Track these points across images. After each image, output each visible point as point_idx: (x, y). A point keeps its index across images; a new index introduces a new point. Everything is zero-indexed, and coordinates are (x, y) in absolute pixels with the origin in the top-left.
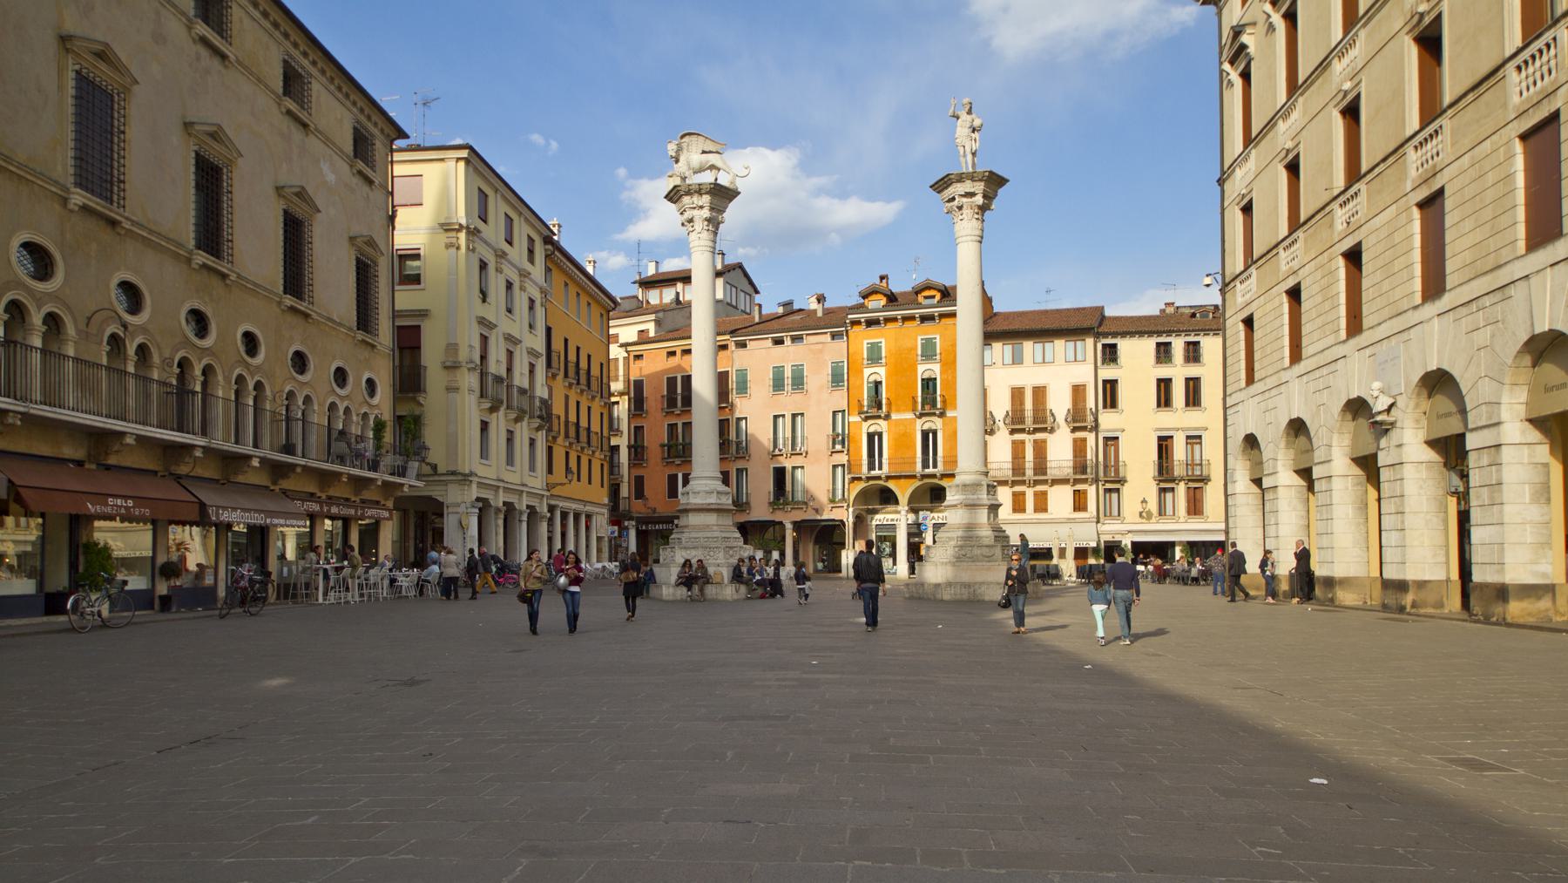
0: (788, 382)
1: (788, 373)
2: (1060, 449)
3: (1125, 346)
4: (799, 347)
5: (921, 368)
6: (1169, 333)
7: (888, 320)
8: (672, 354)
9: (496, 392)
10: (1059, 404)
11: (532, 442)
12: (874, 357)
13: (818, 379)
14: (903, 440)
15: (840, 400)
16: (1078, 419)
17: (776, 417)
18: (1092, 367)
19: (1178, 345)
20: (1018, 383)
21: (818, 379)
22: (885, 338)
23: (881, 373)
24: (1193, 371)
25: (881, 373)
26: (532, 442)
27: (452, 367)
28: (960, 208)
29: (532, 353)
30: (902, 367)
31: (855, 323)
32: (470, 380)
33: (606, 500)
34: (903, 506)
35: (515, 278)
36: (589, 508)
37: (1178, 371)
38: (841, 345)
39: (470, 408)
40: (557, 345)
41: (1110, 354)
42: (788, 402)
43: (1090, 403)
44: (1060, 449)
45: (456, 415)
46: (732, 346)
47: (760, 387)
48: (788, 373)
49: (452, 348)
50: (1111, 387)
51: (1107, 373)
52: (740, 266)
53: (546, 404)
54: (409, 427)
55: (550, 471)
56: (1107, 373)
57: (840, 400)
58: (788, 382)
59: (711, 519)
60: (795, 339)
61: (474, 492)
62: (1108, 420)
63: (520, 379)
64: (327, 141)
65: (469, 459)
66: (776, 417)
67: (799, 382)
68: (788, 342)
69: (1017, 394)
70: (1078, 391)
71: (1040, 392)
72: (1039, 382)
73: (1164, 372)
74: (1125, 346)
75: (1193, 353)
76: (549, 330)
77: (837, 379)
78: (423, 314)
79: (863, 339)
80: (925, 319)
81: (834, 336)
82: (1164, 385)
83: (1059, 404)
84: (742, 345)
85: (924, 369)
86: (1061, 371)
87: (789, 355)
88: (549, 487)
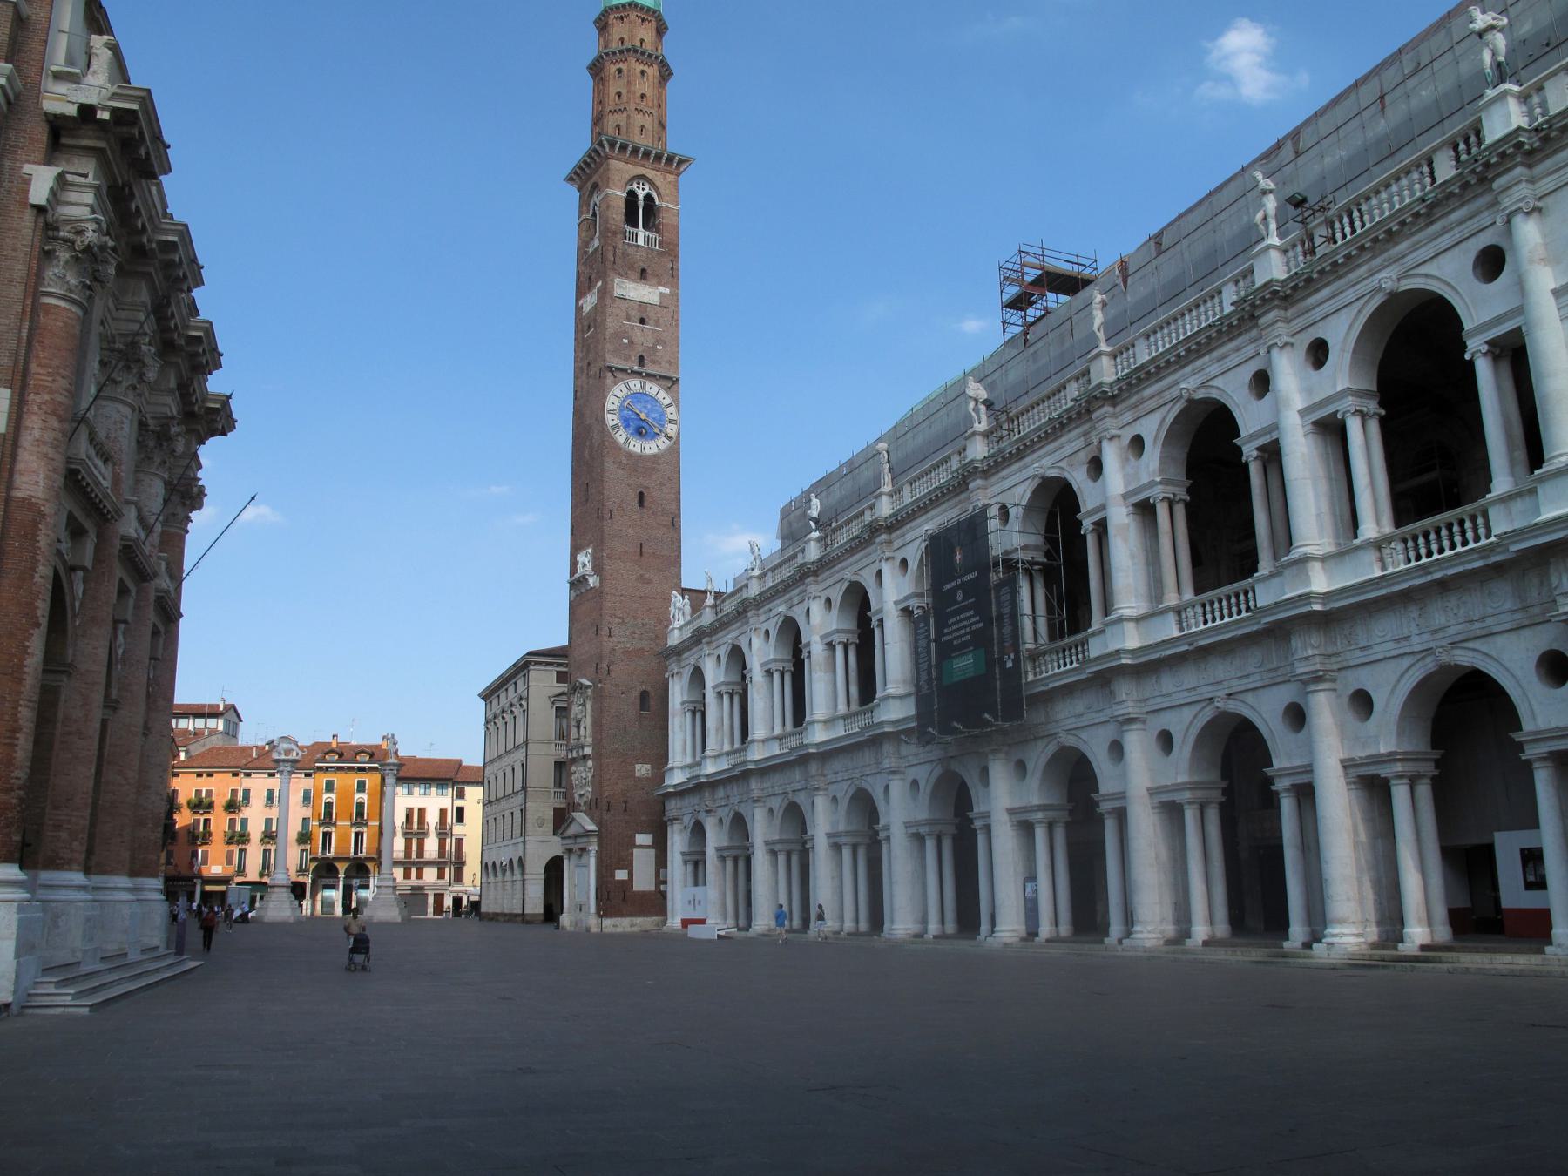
1: (276, 794)
2: (431, 847)
3: (468, 790)
5: (356, 797)
7: (340, 769)
8: (199, 775)
10: (432, 819)
12: (330, 787)
13: (296, 798)
14: (343, 839)
15: (308, 812)
16: (443, 832)
22: (337, 779)
23: (333, 797)
25: (333, 797)
30: (345, 796)
31: (320, 769)
34: (342, 876)
38: (310, 780)
41: (461, 795)
42: (274, 813)
44: (431, 847)
47: (257, 800)
50: (460, 813)
51: (459, 803)
52: (234, 707)
56: (459, 803)
57: (308, 812)
62: (458, 829)
70: (443, 812)
71: (422, 812)
74: (468, 790)
77: (307, 798)
79: (323, 778)
80: (361, 769)
81: (307, 775)
83: (432, 819)
84: (248, 775)
85: (357, 797)
86: (434, 802)
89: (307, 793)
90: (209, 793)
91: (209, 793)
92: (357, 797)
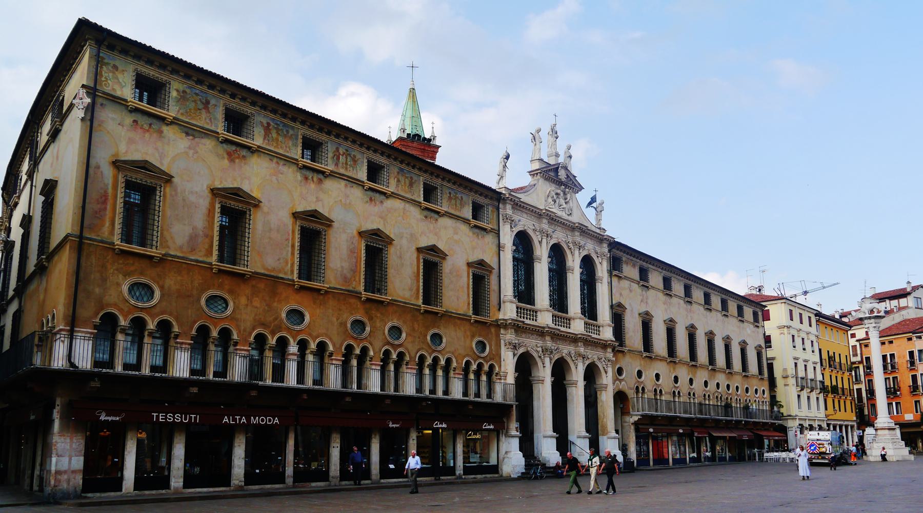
9: (803, 384)
11: (818, 398)
26: (818, 398)
27: (786, 377)
29: (815, 363)
32: (792, 381)
33: (855, 418)
35: (805, 336)
36: (846, 423)
39: (793, 391)
40: (825, 356)
45: (788, 394)
46: (914, 339)
49: (785, 370)
53: (822, 383)
54: (774, 401)
55: (826, 409)
59: (887, 432)
61: (797, 422)
63: (811, 375)
64: (748, 322)
65: (794, 411)
76: (820, 350)
78: (773, 359)
88: (827, 416)
90: (892, 356)
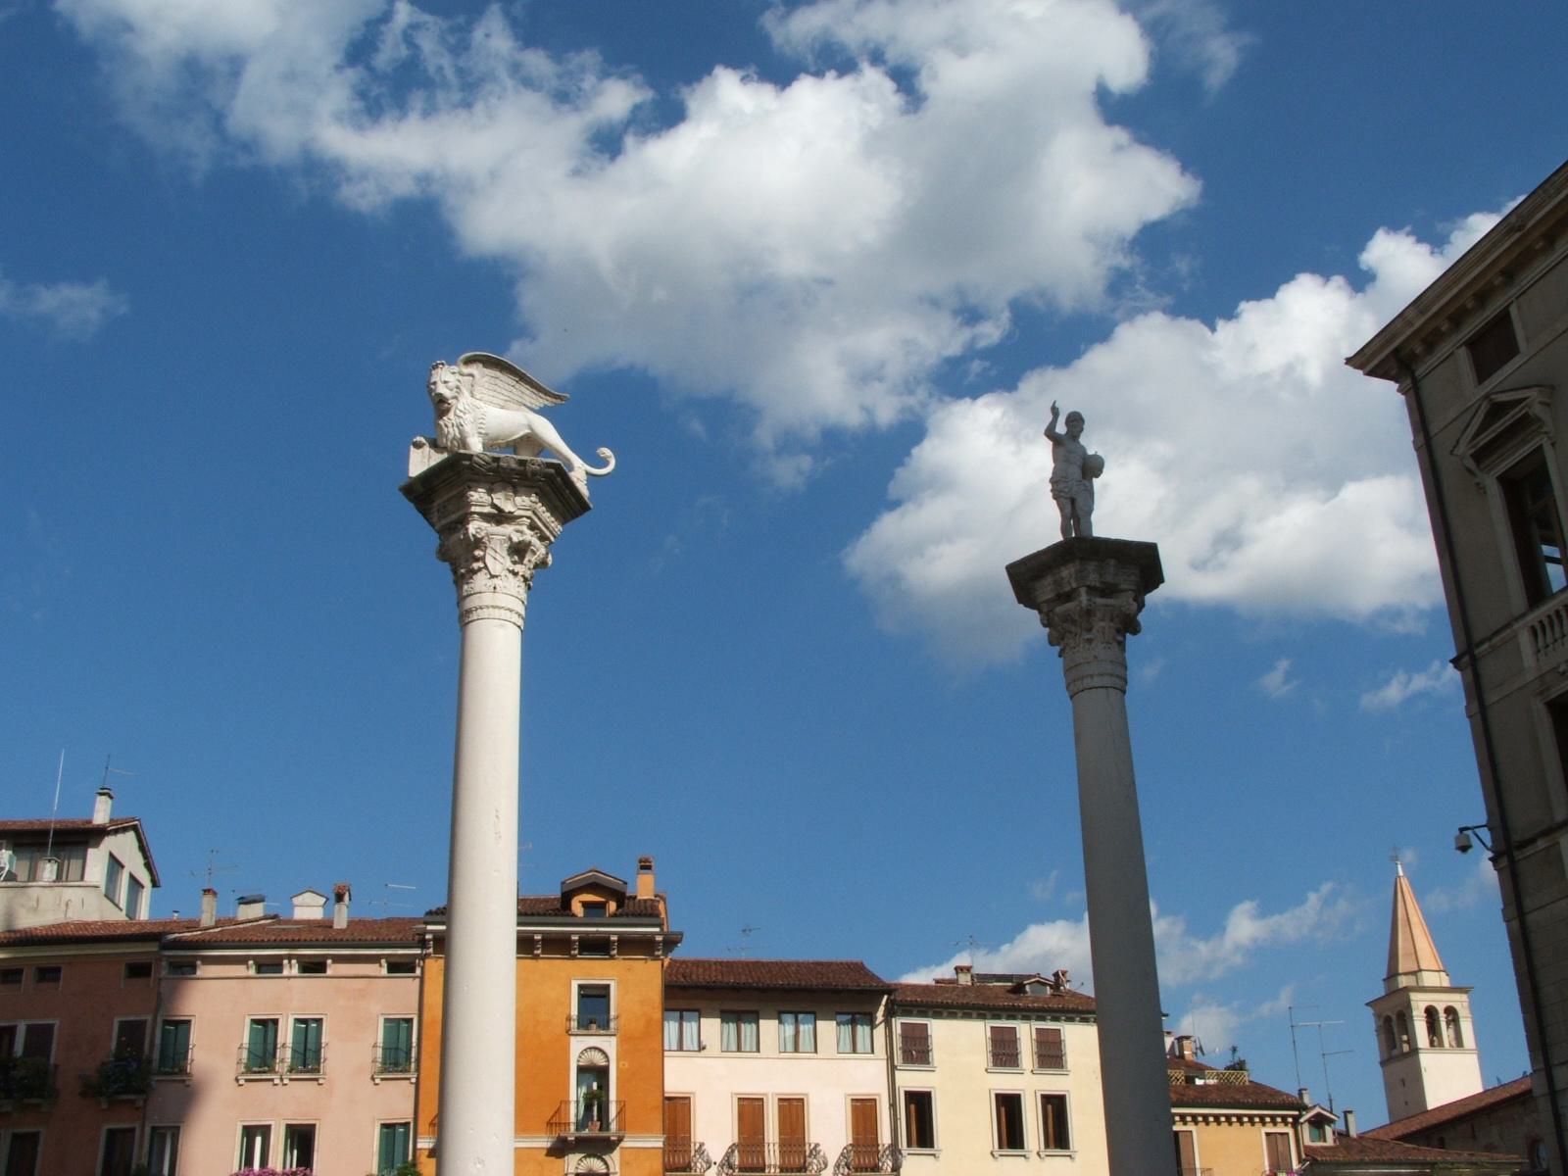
0: (285, 1055)
1: (286, 1035)
4: (313, 984)
6: (1012, 1013)
13: (350, 1050)
17: (250, 1132)
18: (882, 1065)
19: (1026, 1032)
20: (751, 1089)
21: (350, 1050)
24: (1052, 1083)
28: (1089, 613)
37: (1029, 1083)
38: (407, 985)
41: (917, 1050)
42: (282, 1102)
43: (885, 1137)
48: (286, 1035)
50: (920, 1105)
56: (911, 1079)
58: (285, 1055)
60: (313, 967)
66: (250, 1132)
67: (308, 1059)
68: (292, 969)
69: (750, 1111)
70: (863, 1111)
71: (793, 1110)
72: (791, 1090)
73: (1007, 1082)
74: (942, 1031)
75: (1051, 1055)
80: (596, 947)
81: (398, 967)
82: (1009, 1107)
85: (580, 1047)
87: (290, 997)
89: (397, 1028)
90: (40, 1037)
91: (40, 1037)
92: (580, 1047)
